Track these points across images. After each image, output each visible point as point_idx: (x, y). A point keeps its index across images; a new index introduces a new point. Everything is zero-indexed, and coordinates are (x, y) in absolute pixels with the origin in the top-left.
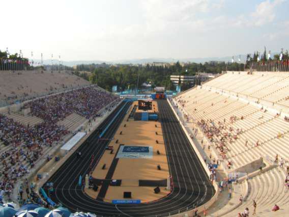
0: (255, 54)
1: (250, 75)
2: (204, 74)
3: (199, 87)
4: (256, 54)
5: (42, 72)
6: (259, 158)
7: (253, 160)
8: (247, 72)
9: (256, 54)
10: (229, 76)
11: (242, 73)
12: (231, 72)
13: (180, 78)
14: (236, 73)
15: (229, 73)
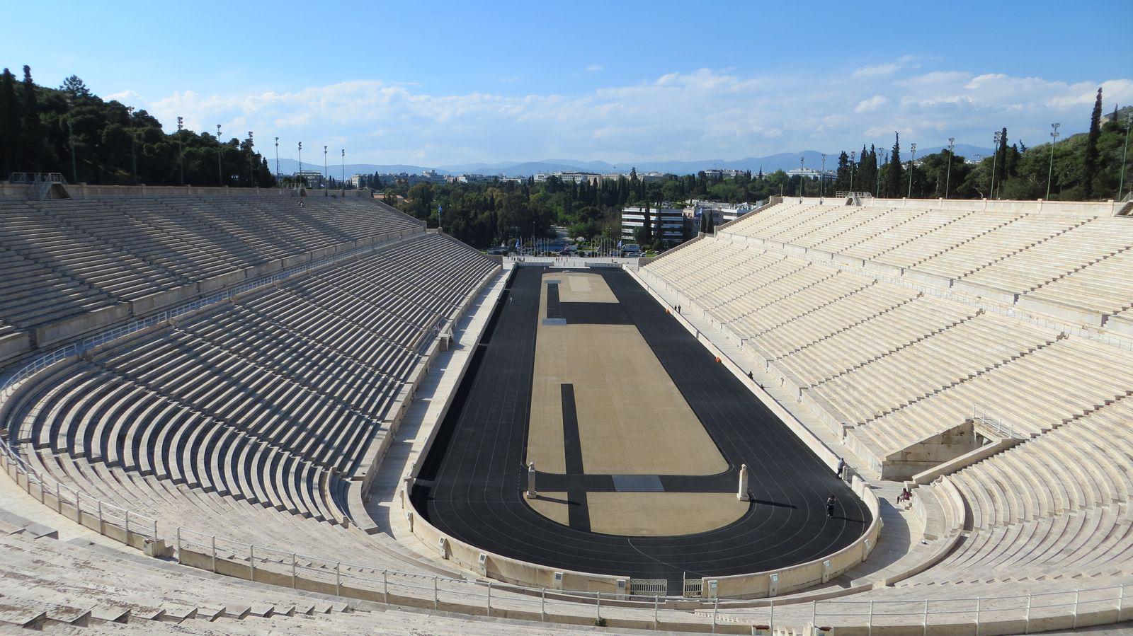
1: (853, 208)
3: (708, 239)
6: (963, 421)
7: (946, 427)
8: (845, 200)
10: (790, 204)
11: (828, 201)
12: (795, 200)
15: (787, 200)
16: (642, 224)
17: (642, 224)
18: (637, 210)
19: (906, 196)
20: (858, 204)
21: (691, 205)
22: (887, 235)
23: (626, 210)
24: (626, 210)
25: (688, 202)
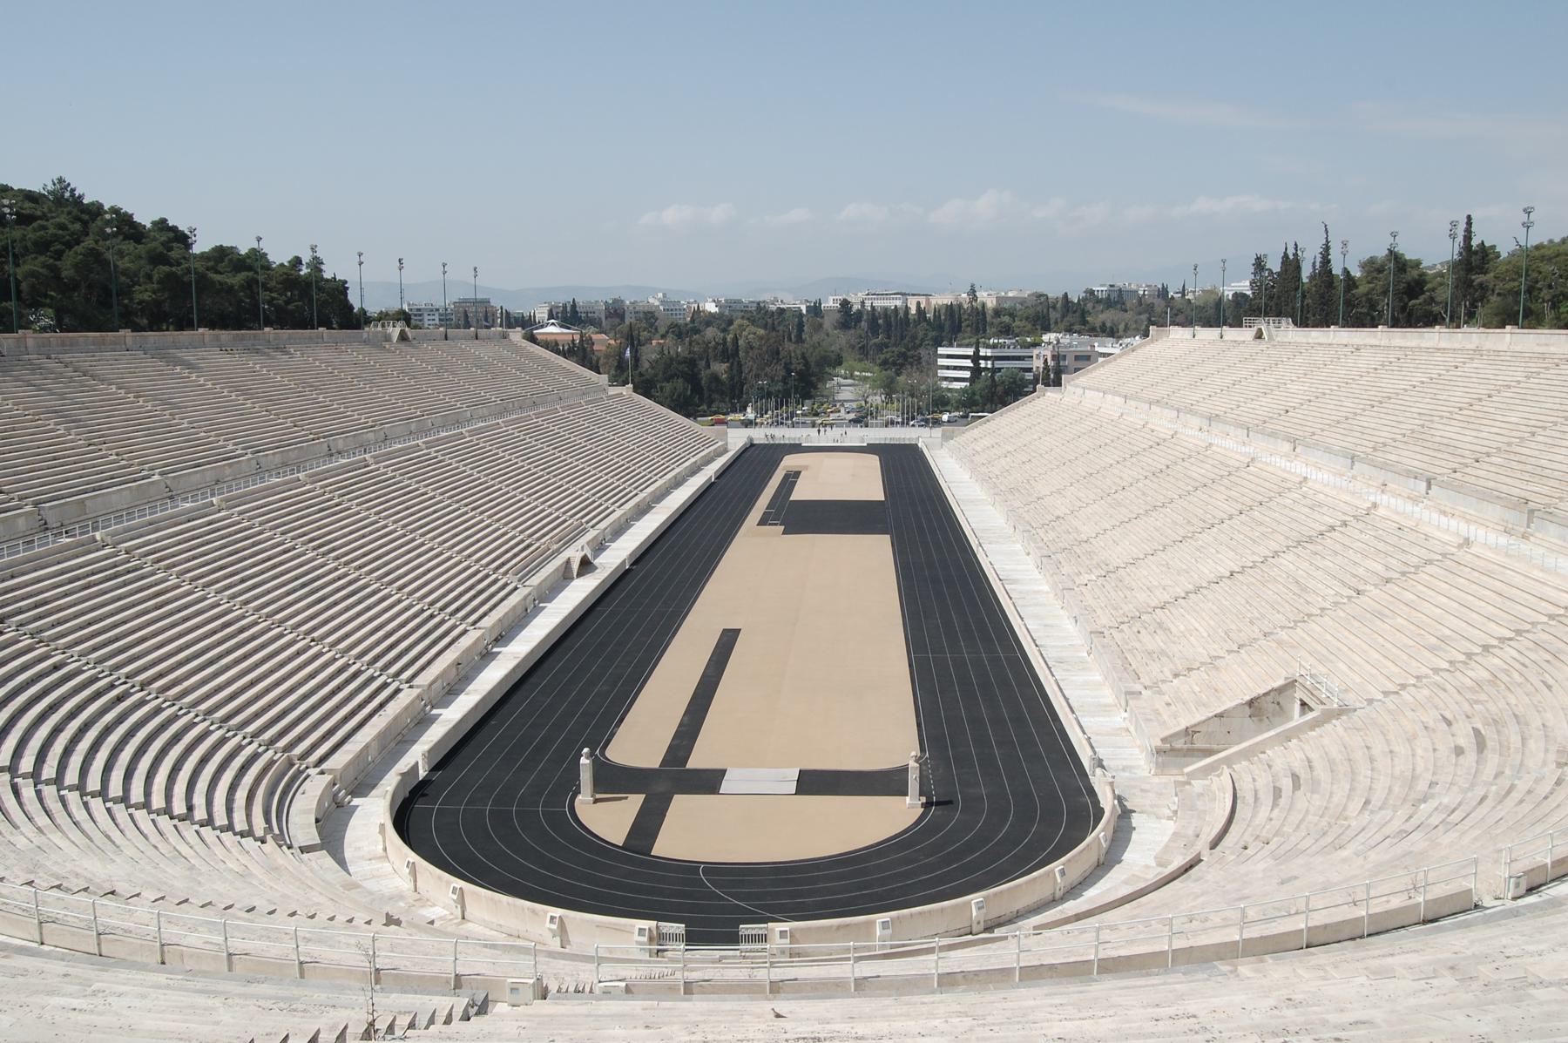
0: (1286, 255)
1: (1262, 345)
2: (1073, 342)
4: (1291, 252)
5: (403, 337)
9: (1291, 252)
11: (1231, 333)
13: (976, 358)
14: (1207, 334)
15: (1178, 334)
19: (1336, 324)
20: (1271, 338)
22: (1293, 387)
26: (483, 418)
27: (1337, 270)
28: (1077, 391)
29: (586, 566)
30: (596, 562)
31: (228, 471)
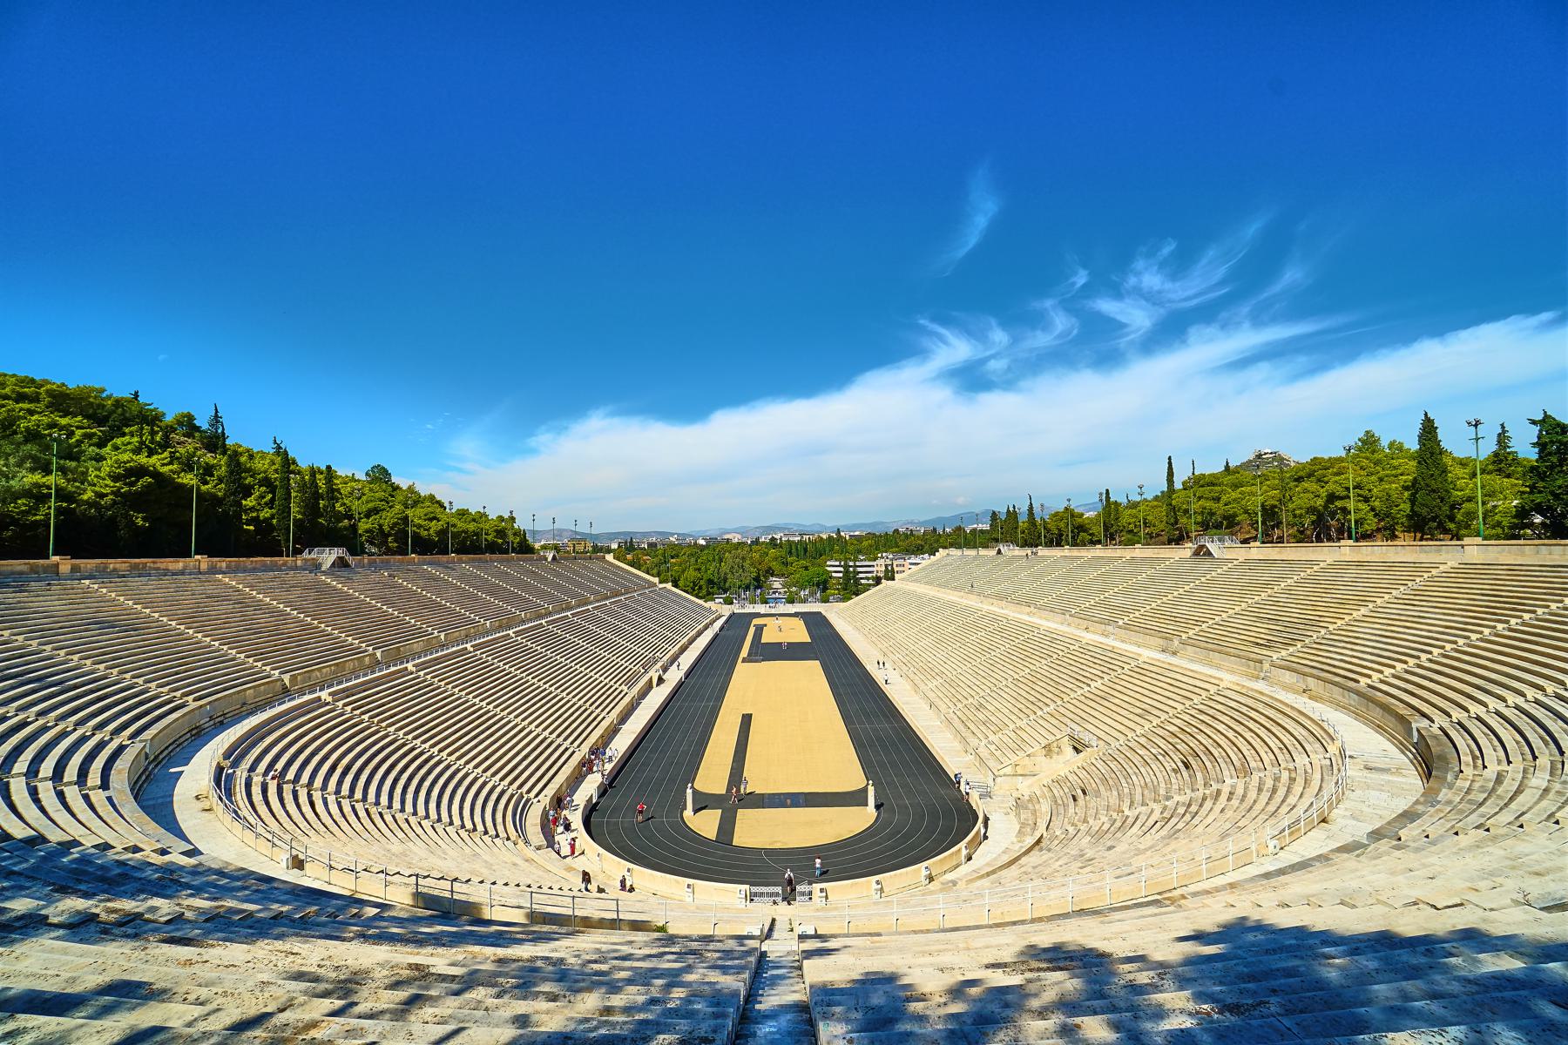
0: (1008, 511)
3: (890, 582)
4: (1011, 509)
9: (1011, 509)
11: (983, 552)
16: (841, 575)
17: (841, 575)
18: (837, 563)
21: (882, 557)
23: (828, 563)
24: (828, 563)
25: (880, 555)
26: (598, 601)
27: (1038, 519)
28: (899, 582)
29: (661, 680)
30: (664, 677)
31: (472, 630)
